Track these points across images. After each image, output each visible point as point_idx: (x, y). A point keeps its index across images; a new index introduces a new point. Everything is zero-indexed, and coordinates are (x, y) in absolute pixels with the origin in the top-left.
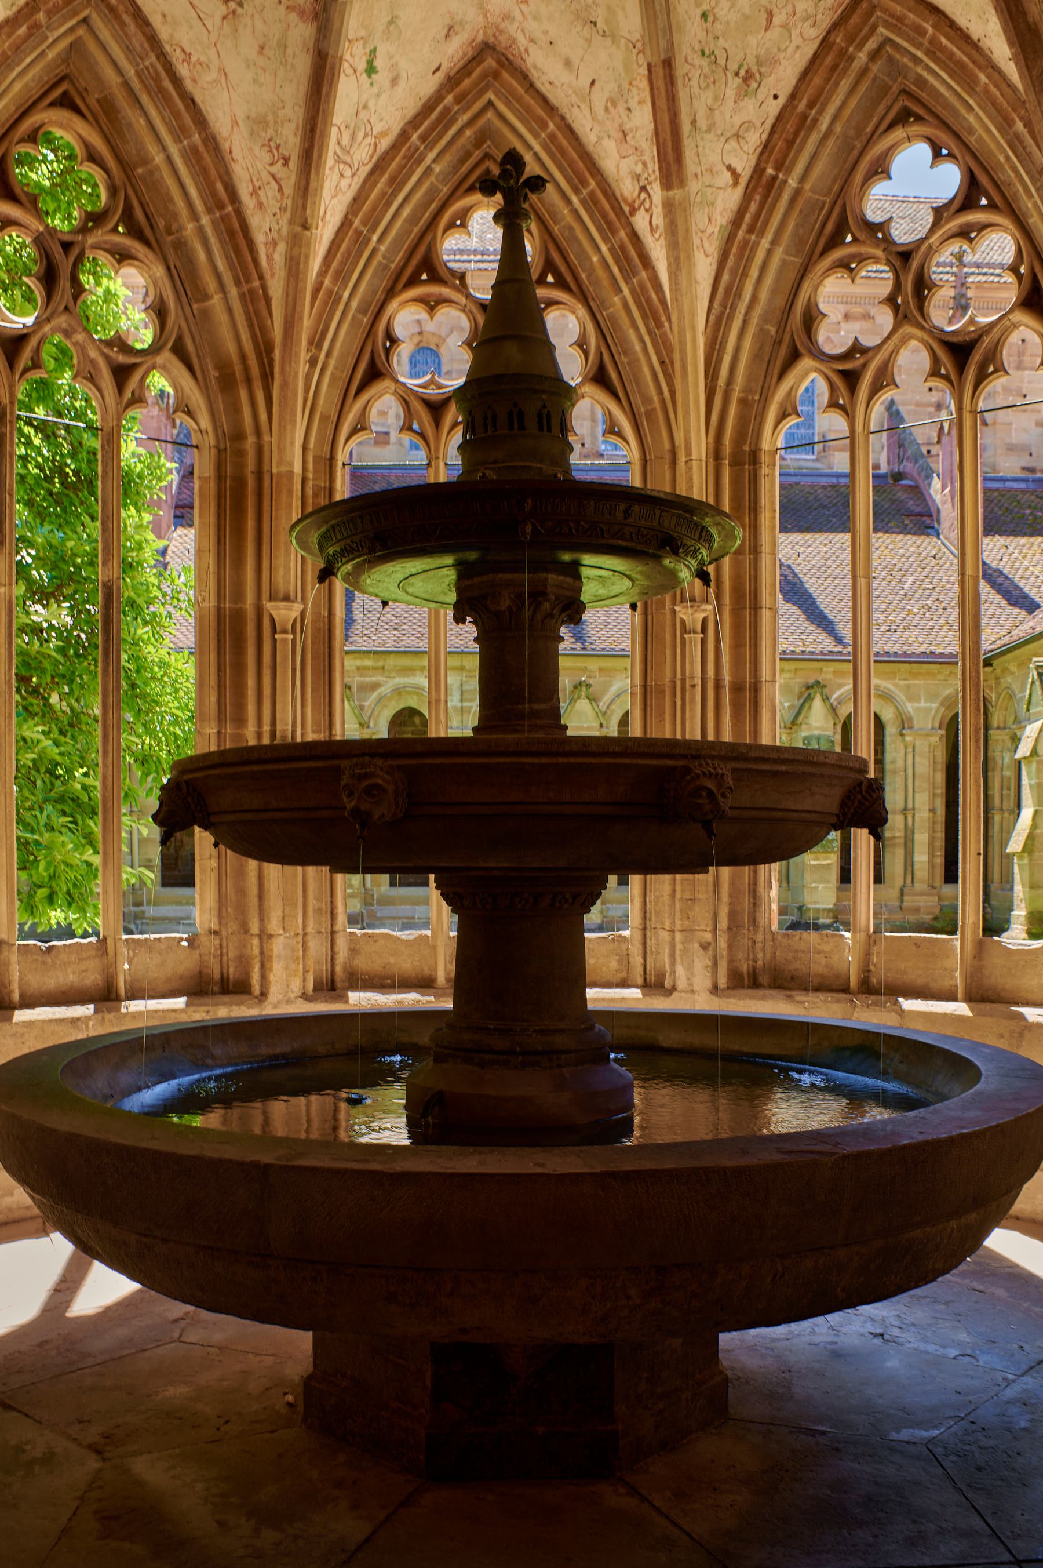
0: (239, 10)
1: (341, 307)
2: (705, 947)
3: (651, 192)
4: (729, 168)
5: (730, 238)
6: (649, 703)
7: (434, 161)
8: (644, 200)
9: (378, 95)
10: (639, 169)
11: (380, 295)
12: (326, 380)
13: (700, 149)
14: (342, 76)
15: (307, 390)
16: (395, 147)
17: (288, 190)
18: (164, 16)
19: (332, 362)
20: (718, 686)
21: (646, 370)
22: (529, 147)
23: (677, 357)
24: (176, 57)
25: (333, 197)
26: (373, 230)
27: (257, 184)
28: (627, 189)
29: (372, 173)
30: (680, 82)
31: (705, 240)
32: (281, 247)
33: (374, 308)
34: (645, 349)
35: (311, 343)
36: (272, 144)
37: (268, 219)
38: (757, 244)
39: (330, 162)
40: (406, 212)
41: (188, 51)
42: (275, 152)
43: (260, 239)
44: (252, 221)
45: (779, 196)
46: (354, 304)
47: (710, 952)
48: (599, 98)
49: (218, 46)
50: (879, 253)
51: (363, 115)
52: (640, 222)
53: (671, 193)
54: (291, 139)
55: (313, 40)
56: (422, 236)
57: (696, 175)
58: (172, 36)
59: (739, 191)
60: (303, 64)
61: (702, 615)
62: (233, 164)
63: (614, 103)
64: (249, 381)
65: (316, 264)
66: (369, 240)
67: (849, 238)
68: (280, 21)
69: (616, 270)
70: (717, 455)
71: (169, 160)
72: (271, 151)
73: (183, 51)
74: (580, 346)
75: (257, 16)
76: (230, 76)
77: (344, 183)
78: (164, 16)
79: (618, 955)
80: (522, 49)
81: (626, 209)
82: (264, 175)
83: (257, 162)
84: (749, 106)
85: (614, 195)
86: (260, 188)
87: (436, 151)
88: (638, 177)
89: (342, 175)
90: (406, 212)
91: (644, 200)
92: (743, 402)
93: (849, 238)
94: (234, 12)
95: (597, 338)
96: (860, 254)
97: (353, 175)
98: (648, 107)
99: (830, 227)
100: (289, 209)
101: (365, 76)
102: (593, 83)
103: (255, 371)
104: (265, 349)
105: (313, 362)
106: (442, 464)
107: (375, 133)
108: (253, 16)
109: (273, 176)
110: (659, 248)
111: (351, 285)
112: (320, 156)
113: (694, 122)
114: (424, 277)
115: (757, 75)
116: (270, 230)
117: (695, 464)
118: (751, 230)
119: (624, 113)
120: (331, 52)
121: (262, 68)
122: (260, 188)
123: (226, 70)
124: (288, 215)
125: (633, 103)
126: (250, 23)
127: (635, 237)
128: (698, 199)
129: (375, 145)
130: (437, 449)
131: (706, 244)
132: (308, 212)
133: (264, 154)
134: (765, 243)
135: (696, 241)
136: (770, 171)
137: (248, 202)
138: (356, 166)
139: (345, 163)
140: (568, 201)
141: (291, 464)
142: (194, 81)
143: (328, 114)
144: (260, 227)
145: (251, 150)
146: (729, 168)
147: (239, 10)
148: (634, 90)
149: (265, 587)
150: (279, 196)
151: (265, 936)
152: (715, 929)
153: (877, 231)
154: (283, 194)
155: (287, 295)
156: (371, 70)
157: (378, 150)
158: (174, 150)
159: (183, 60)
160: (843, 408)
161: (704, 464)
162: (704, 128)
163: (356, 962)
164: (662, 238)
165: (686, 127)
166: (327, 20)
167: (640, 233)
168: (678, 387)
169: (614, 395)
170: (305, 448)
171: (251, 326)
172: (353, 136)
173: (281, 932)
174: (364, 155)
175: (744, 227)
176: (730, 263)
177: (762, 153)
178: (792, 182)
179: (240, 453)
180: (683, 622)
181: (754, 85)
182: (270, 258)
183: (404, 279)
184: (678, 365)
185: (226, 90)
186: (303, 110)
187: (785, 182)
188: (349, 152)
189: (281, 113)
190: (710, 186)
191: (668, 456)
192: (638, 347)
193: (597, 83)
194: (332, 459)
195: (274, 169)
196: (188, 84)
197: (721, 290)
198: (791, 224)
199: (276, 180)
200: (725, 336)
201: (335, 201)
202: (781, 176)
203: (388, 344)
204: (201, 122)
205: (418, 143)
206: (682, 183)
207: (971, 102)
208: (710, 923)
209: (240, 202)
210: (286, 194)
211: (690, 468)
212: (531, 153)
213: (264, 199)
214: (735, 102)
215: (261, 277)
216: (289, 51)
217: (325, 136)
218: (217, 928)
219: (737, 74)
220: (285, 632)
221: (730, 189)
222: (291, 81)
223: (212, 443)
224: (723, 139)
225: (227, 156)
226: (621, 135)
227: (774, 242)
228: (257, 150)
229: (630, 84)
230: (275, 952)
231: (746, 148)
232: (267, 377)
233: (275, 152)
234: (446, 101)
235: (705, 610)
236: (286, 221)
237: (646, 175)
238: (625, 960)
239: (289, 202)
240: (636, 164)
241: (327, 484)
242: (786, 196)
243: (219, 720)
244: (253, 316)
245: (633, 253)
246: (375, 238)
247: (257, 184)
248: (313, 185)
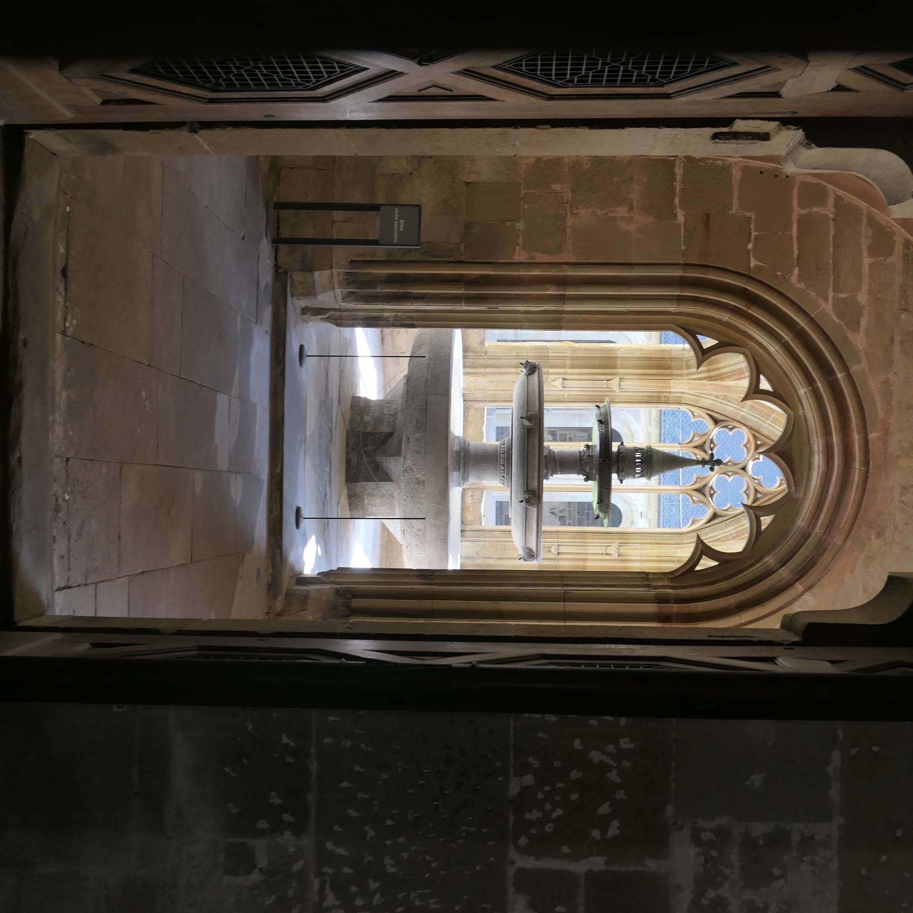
1: (740, 408)
2: (477, 553)
6: (580, 534)
11: (749, 424)
19: (718, 404)
20: (584, 560)
21: (716, 534)
33: (744, 422)
34: (725, 533)
35: (724, 396)
46: (743, 413)
47: (475, 556)
61: (613, 553)
64: (709, 371)
74: (729, 508)
79: (474, 520)
103: (712, 374)
104: (721, 378)
105: (717, 397)
106: (679, 449)
111: (749, 412)
130: (685, 447)
141: (673, 388)
149: (625, 377)
151: (485, 374)
152: (484, 558)
155: (739, 387)
163: (472, 410)
169: (709, 522)
170: (683, 393)
171: (730, 372)
173: (487, 381)
179: (681, 368)
180: (611, 546)
183: (756, 434)
191: (680, 542)
192: (726, 530)
194: (681, 403)
208: (487, 555)
218: (488, 354)
220: (607, 385)
223: (685, 356)
230: (478, 378)
232: (710, 378)
235: (615, 554)
238: (472, 523)
241: (670, 402)
243: (572, 357)
244: (734, 373)
246: (768, 422)
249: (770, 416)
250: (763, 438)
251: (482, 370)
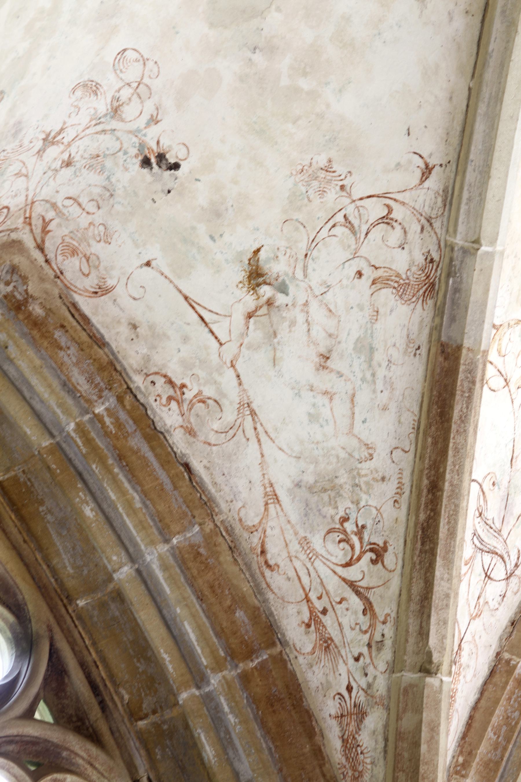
0: (281, 299)
18: (135, 327)
25: (473, 618)
27: (319, 605)
36: (349, 527)
37: (342, 669)
41: (178, 383)
42: (355, 540)
44: (309, 675)
49: (239, 366)
55: (426, 331)
58: (147, 359)
62: (268, 573)
68: (361, 308)
72: (346, 540)
73: (170, 382)
75: (314, 306)
76: (262, 416)
78: (135, 327)
83: (318, 563)
86: (324, 612)
94: (270, 303)
100: (388, 643)
108: (306, 304)
109: (352, 585)
116: (349, 689)
120: (467, 343)
121: (326, 393)
122: (324, 612)
123: (254, 406)
124: (387, 654)
126: (301, 318)
133: (331, 547)
142: (191, 432)
144: (327, 686)
145: (305, 542)
147: (281, 299)
150: (364, 621)
154: (374, 615)
159: (170, 399)
166: (457, 290)
185: (253, 440)
186: (411, 455)
189: (366, 467)
199: (358, 593)
201: (477, 624)
209: (284, 643)
210: (381, 614)
213: (333, 631)
216: (379, 356)
222: (385, 408)
225: (256, 560)
233: (355, 540)
236: (382, 666)
239: (388, 630)
247: (319, 605)
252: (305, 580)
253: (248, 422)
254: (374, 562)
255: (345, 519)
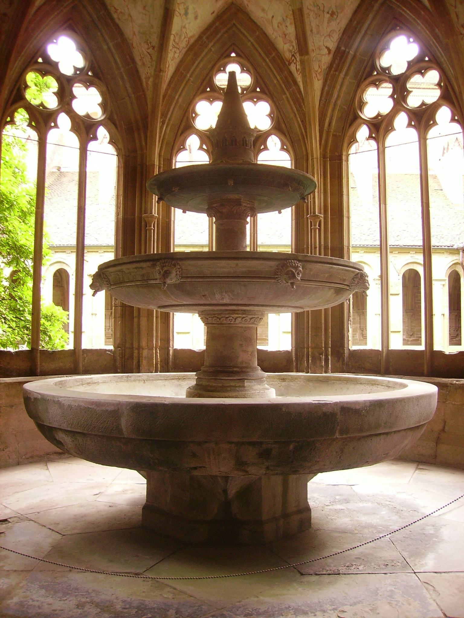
3: (296, 57)
4: (326, 47)
5: (328, 74)
7: (212, 47)
8: (294, 60)
9: (189, 23)
10: (291, 48)
12: (169, 129)
13: (314, 41)
14: (175, 17)
15: (160, 133)
16: (196, 41)
17: (154, 58)
22: (249, 41)
23: (307, 119)
24: (112, 10)
26: (188, 72)
28: (288, 55)
29: (188, 51)
30: (305, 16)
31: (317, 74)
32: (151, 80)
38: (339, 75)
39: (170, 48)
40: (201, 65)
43: (143, 77)
45: (347, 57)
48: (275, 22)
50: (387, 79)
51: (184, 30)
52: (293, 68)
53: (303, 57)
54: (155, 40)
56: (207, 75)
57: (313, 50)
59: (331, 56)
60: (160, 12)
62: (133, 49)
63: (281, 24)
65: (164, 86)
66: (186, 76)
67: (375, 73)
69: (283, 86)
70: (324, 156)
71: (109, 48)
73: (115, 8)
77: (177, 55)
80: (246, 5)
81: (287, 63)
82: (145, 53)
84: (334, 24)
85: (282, 57)
86: (143, 58)
87: (212, 43)
88: (291, 51)
89: (175, 52)
90: (201, 65)
91: (294, 60)
92: (335, 136)
93: (375, 73)
95: (276, 112)
96: (380, 79)
97: (180, 52)
98: (293, 26)
99: (368, 69)
101: (184, 16)
102: (273, 17)
105: (163, 123)
107: (188, 37)
110: (299, 78)
111: (179, 93)
112: (166, 45)
113: (311, 31)
114: (208, 89)
115: (336, 13)
117: (315, 160)
118: (336, 71)
119: (284, 28)
125: (288, 24)
127: (291, 73)
128: (314, 59)
129: (189, 40)
131: (318, 76)
132: (162, 66)
134: (342, 75)
135: (314, 75)
136: (343, 48)
137: (139, 63)
138: (181, 48)
139: (177, 48)
140: (264, 60)
143: (170, 31)
145: (140, 44)
146: (326, 47)
148: (288, 19)
153: (386, 71)
156: (186, 14)
157: (190, 43)
158: (111, 45)
160: (374, 138)
161: (319, 160)
162: (315, 32)
164: (301, 74)
165: (308, 33)
167: (293, 72)
168: (308, 130)
170: (160, 155)
172: (180, 37)
174: (184, 45)
175: (333, 69)
176: (328, 83)
177: (340, 41)
178: (352, 53)
181: (335, 17)
182: (147, 84)
184: (308, 123)
187: (349, 52)
188: (178, 44)
190: (319, 54)
193: (274, 17)
195: (149, 51)
196: (117, 21)
197: (325, 93)
198: (352, 68)
199: (149, 55)
200: (327, 110)
201: (173, 62)
202: (347, 50)
203: (194, 115)
204: (121, 34)
205: (205, 40)
206: (307, 53)
207: (419, 21)
211: (313, 161)
212: (250, 43)
213: (145, 62)
214: (328, 23)
215: (144, 91)
217: (168, 38)
219: (328, 13)
221: (327, 55)
224: (323, 37)
226: (284, 36)
227: (346, 75)
228: (142, 44)
229: (287, 17)
231: (333, 40)
232: (146, 128)
234: (217, 25)
237: (294, 50)
240: (290, 47)
242: (350, 58)
245: (290, 80)
248: (164, 56)
249: (182, 73)
250: (204, 84)
251: (136, 352)
252: (140, 51)
253: (130, 19)
254: (153, 49)
255: (148, 40)
